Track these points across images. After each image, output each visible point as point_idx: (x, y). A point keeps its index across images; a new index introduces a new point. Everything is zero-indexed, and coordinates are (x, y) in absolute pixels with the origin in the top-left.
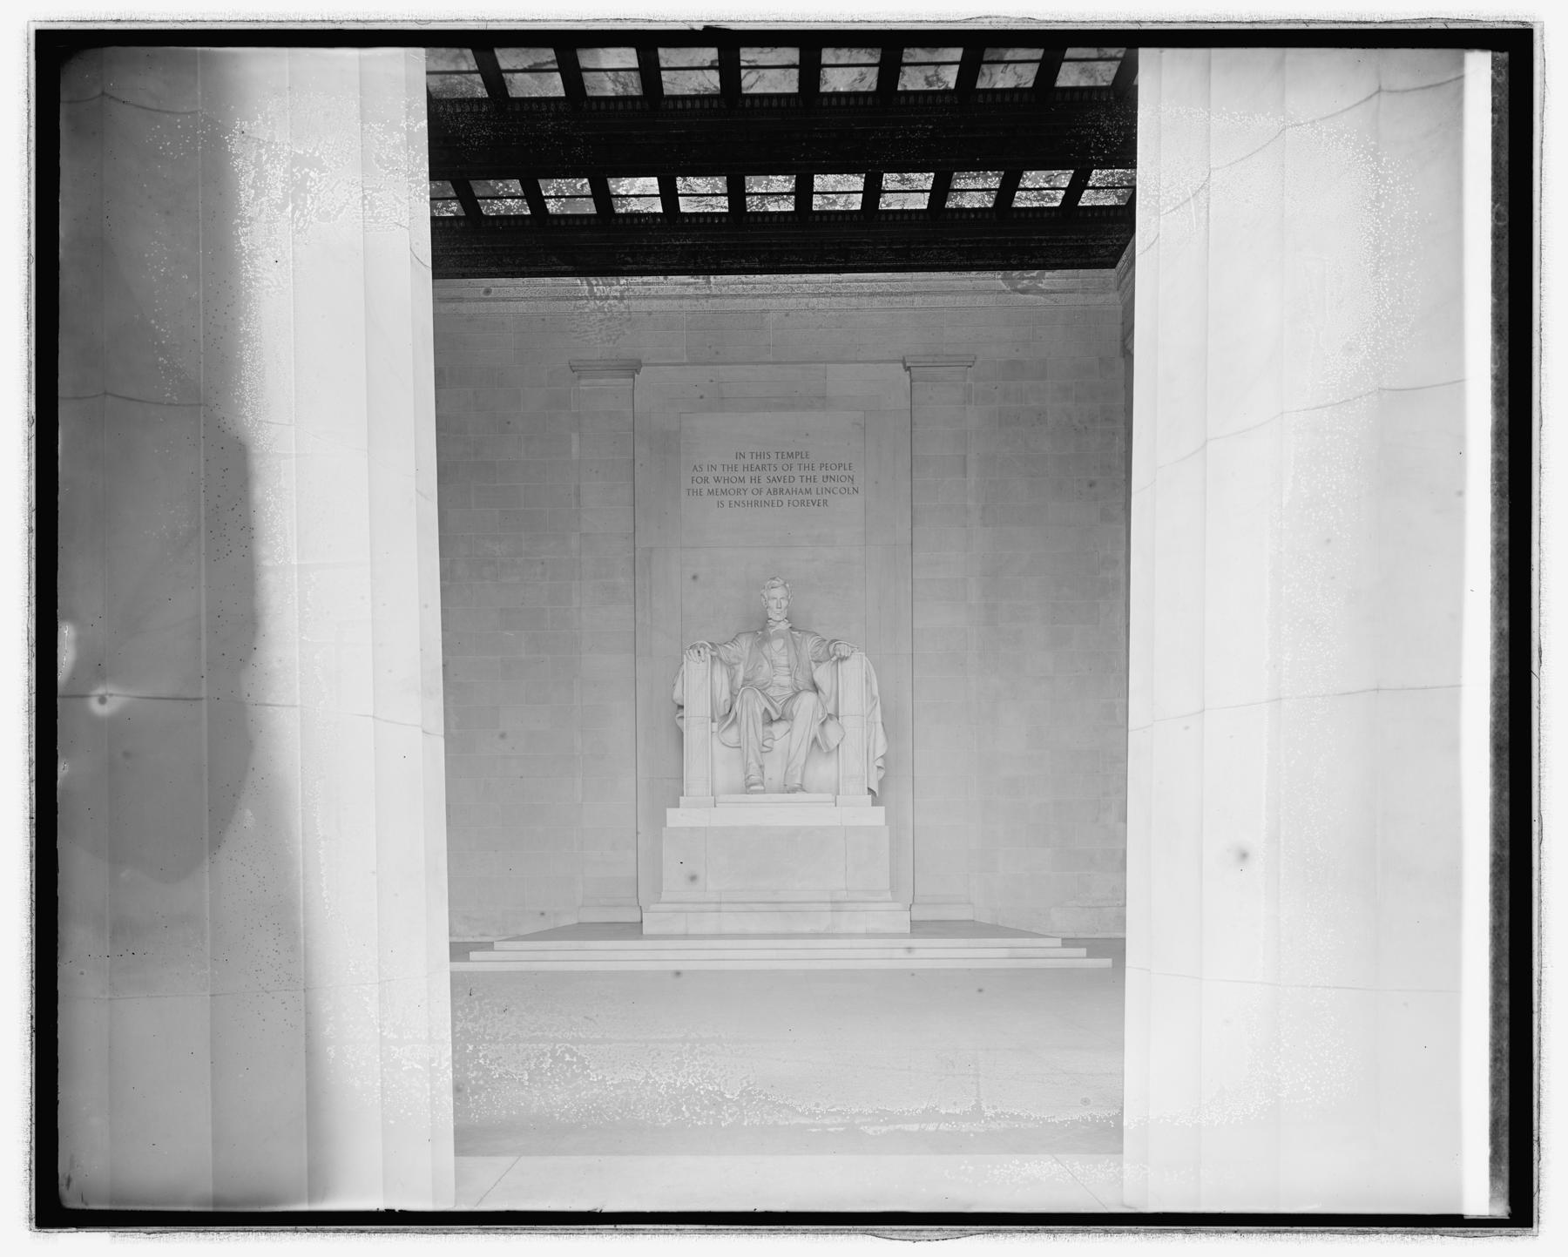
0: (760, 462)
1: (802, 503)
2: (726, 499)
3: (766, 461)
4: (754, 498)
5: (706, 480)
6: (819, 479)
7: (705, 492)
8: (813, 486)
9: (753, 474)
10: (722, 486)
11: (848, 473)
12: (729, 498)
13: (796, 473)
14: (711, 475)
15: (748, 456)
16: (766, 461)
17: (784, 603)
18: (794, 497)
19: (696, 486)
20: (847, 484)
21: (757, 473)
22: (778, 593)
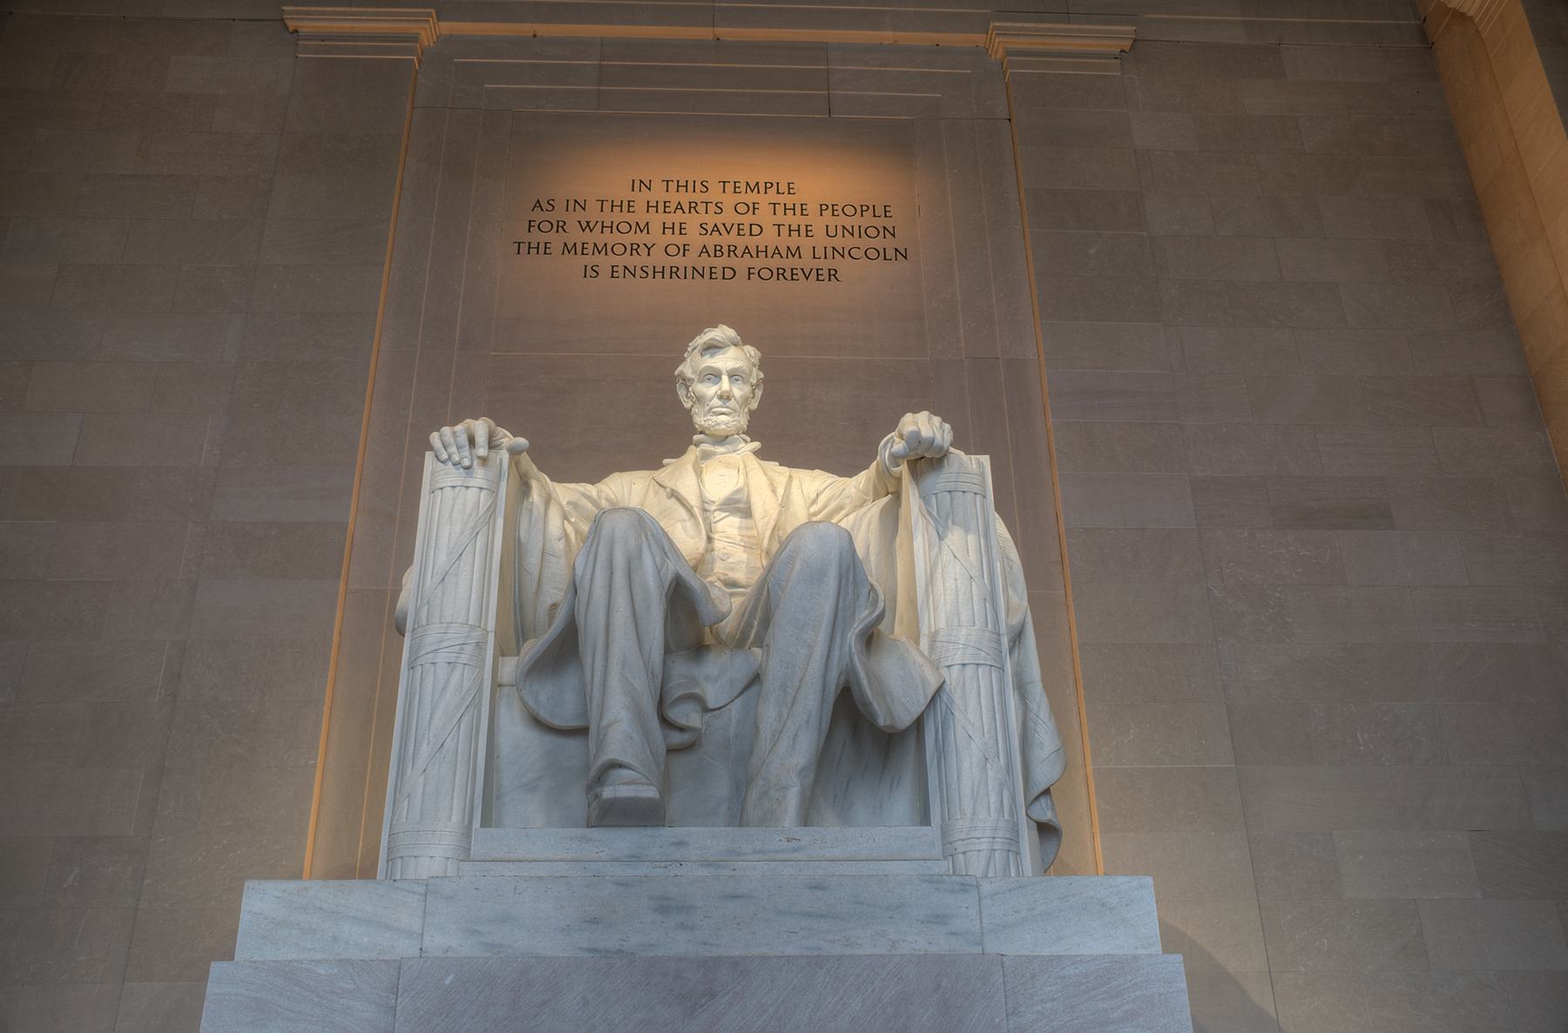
0: (685, 198)
3: (698, 197)
4: (669, 262)
5: (561, 226)
6: (818, 230)
7: (556, 247)
8: (806, 244)
9: (669, 219)
11: (880, 222)
14: (572, 219)
15: (658, 186)
17: (738, 391)
18: (757, 263)
19: (537, 237)
20: (889, 243)
21: (678, 217)
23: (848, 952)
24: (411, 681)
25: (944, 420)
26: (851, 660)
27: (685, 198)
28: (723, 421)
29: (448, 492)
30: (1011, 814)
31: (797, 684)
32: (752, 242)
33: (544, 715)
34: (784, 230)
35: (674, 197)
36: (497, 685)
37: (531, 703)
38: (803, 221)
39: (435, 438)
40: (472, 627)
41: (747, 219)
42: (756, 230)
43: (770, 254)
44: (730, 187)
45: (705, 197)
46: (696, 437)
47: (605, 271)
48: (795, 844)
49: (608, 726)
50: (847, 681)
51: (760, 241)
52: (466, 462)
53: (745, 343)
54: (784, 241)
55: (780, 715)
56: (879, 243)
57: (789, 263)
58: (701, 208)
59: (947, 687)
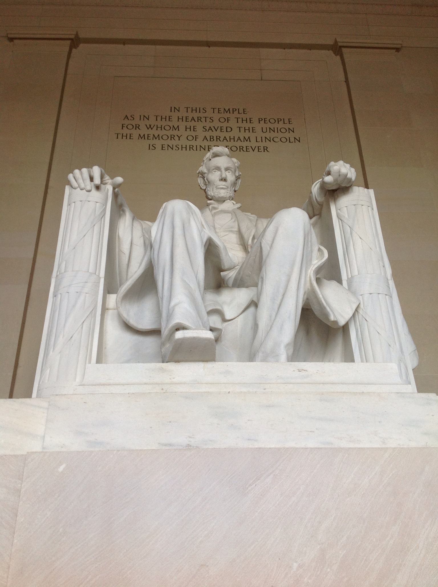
0: (196, 115)
1: (241, 148)
2: (158, 143)
3: (201, 115)
4: (189, 143)
6: (258, 129)
8: (253, 136)
9: (189, 124)
10: (154, 132)
11: (287, 126)
12: (162, 142)
13: (232, 123)
14: (142, 124)
16: (201, 115)
17: (230, 177)
19: (125, 131)
20: (291, 135)
21: (193, 124)
22: (223, 162)
23: (352, 445)
24: (54, 304)
25: (351, 166)
26: (311, 284)
27: (196, 115)
28: (223, 193)
29: (78, 204)
30: (407, 377)
31: (280, 298)
32: (228, 135)
33: (133, 322)
34: (242, 130)
35: (190, 115)
36: (104, 309)
37: (125, 315)
38: (251, 125)
39: (71, 177)
40: (91, 273)
41: (225, 125)
42: (229, 129)
43: (236, 139)
44: (216, 111)
45: (205, 115)
46: (209, 202)
47: (159, 147)
48: (303, 373)
49: (176, 305)
50: (307, 299)
51: (232, 134)
52: (88, 188)
53: (231, 157)
54: (242, 135)
55: (270, 316)
56: (287, 135)
57: (245, 144)
58: (203, 120)
59: (362, 306)
